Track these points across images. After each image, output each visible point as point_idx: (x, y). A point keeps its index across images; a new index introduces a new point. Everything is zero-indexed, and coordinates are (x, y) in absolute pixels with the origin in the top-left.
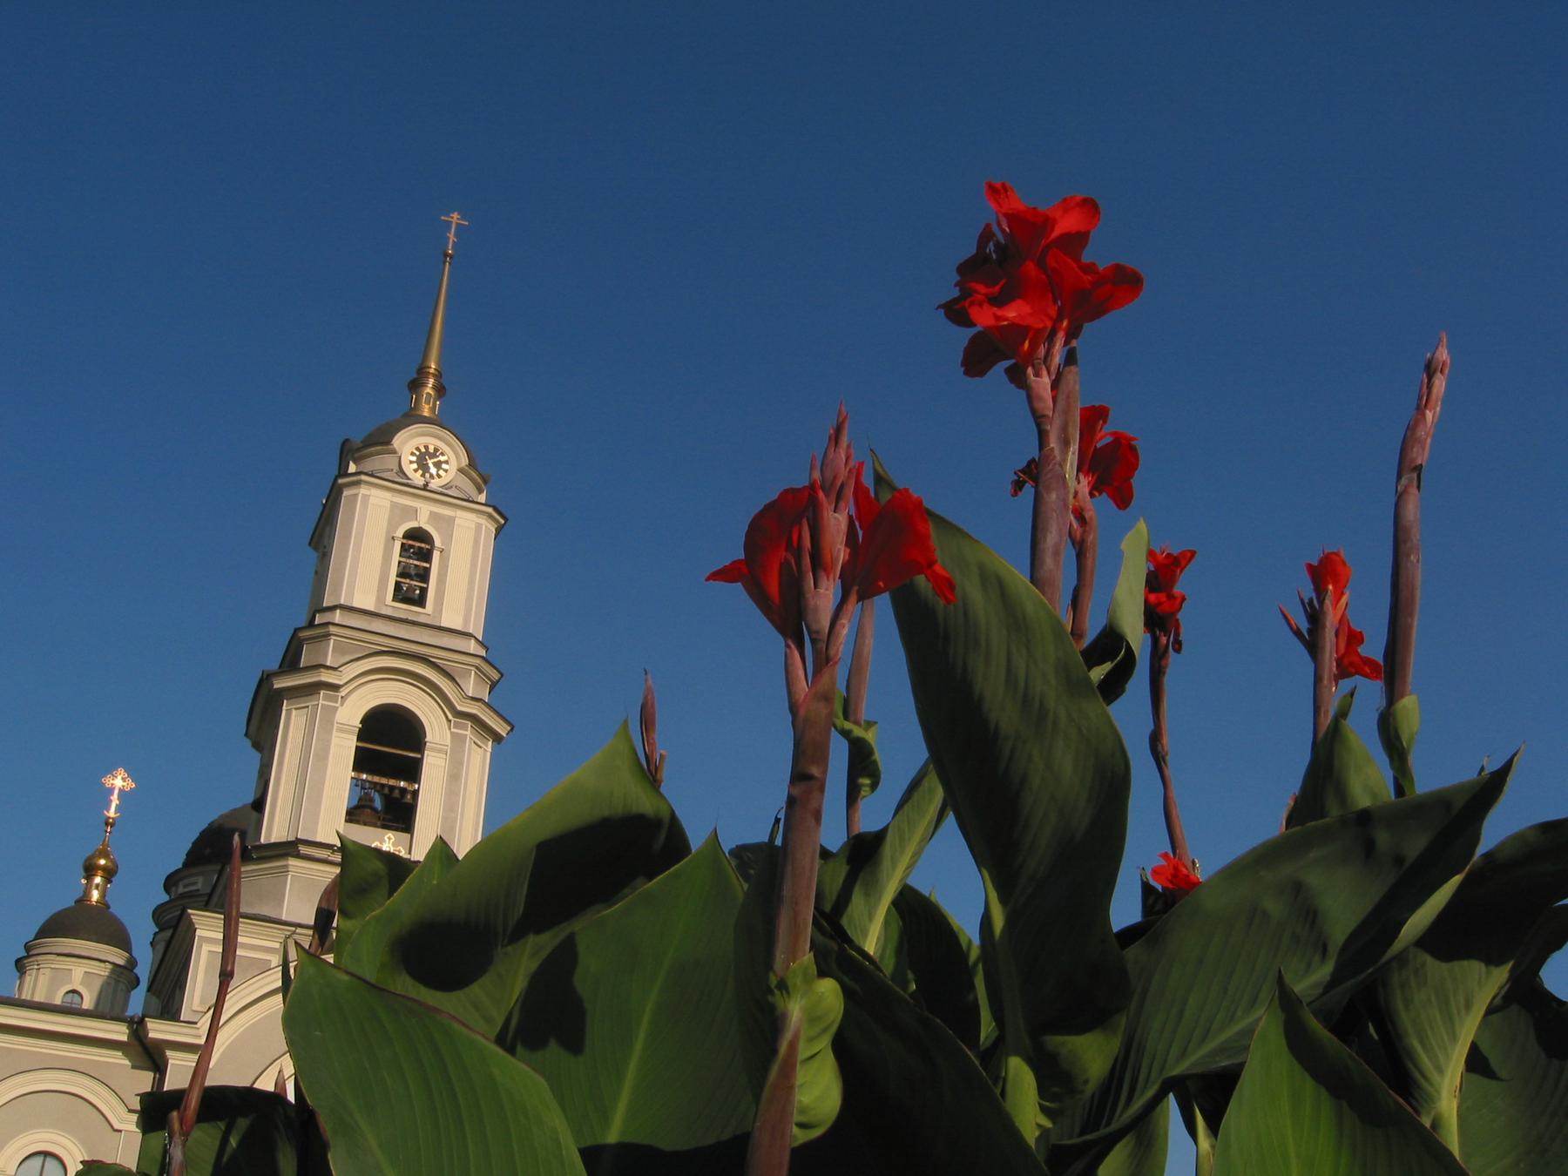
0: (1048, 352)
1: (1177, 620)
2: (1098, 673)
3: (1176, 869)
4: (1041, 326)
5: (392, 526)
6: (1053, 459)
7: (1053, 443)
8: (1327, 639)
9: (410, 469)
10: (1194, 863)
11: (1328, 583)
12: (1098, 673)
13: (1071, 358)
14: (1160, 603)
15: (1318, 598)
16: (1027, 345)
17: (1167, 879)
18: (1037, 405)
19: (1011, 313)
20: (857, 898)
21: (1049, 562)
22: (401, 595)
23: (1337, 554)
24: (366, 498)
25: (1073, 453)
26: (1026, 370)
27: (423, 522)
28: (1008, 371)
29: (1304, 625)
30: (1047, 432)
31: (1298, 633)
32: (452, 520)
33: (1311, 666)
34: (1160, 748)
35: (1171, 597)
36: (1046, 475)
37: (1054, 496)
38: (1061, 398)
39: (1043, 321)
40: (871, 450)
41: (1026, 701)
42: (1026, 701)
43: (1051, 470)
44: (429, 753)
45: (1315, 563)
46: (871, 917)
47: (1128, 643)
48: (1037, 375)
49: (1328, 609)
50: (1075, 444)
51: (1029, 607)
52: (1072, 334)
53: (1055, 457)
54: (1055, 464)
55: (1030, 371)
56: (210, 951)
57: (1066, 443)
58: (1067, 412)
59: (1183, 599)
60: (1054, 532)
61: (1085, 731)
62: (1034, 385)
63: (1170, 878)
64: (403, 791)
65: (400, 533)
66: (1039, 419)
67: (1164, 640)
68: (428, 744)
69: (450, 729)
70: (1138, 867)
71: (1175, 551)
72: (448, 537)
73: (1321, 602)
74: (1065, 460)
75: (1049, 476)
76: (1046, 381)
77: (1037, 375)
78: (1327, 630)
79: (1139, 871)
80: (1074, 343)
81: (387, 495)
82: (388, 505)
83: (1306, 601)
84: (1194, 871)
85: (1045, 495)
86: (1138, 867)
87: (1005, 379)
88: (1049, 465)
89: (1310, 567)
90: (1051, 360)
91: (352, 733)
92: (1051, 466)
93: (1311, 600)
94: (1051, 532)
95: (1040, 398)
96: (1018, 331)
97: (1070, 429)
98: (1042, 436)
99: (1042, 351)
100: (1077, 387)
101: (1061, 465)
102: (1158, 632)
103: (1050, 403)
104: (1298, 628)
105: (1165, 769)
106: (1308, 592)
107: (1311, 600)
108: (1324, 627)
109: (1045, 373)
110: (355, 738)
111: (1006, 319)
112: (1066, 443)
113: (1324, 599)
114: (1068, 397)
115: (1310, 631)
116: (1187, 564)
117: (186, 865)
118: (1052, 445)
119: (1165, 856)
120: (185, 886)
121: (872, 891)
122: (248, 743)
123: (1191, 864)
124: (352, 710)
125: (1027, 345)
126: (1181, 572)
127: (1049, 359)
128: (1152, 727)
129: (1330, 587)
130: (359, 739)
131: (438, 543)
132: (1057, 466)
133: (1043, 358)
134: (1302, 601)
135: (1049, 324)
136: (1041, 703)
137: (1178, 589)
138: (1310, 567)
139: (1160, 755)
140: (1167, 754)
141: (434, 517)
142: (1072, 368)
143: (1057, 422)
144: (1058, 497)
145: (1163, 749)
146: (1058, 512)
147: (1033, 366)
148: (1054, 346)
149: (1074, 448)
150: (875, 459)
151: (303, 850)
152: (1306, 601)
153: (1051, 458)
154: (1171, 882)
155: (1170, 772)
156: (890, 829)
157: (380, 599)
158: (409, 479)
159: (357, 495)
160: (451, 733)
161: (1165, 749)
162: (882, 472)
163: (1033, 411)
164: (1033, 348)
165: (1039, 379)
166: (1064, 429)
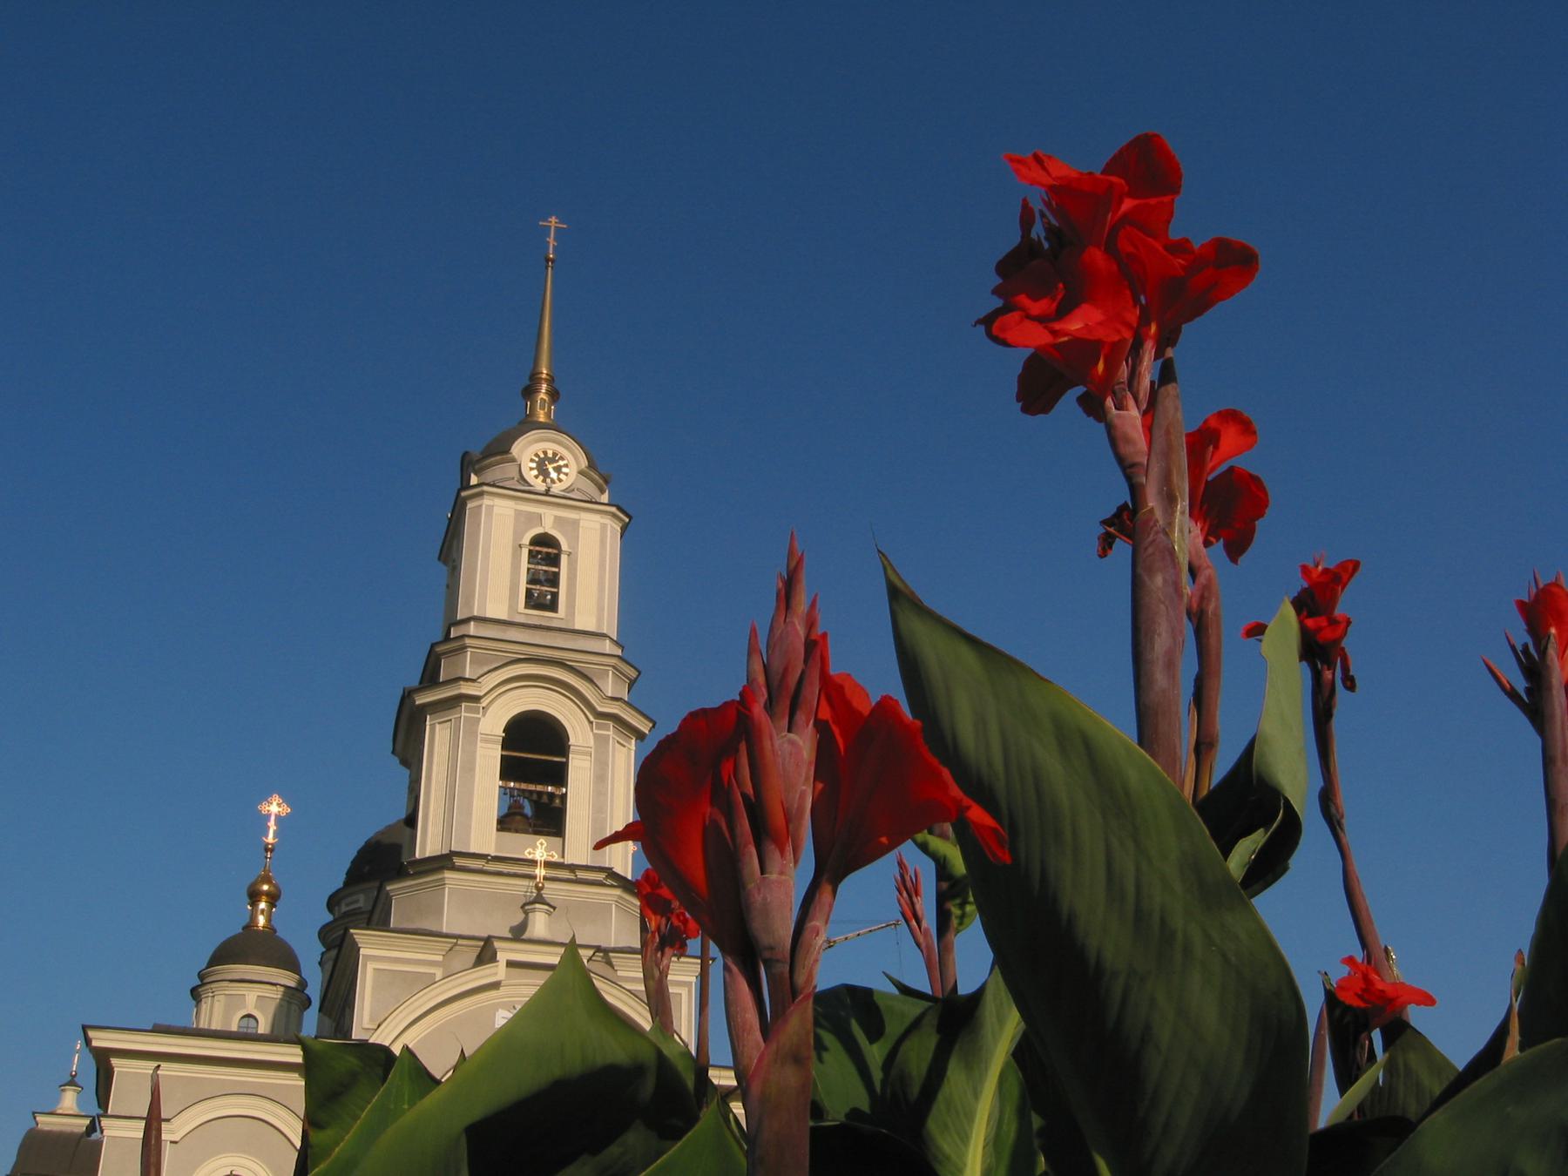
0: (1134, 374)
1: (1343, 649)
2: (1247, 848)
3: (1366, 978)
4: (1116, 338)
5: (518, 534)
6: (1152, 528)
7: (1153, 501)
8: (1557, 704)
9: (531, 475)
10: (1386, 950)
11: (1551, 625)
12: (1247, 848)
13: (1167, 374)
14: (1319, 629)
15: (1537, 645)
16: (1101, 366)
17: (1356, 994)
18: (1126, 450)
19: (1074, 325)
20: (955, 1074)
21: (1160, 678)
22: (533, 602)
23: (1556, 584)
24: (490, 508)
25: (1183, 513)
26: (1105, 400)
27: (548, 527)
28: (1082, 401)
29: (1521, 685)
30: (1142, 486)
31: (1512, 694)
32: (576, 523)
33: (1537, 741)
34: (1333, 810)
35: (1333, 622)
36: (1146, 549)
37: (1159, 580)
38: (1158, 434)
39: (1119, 332)
40: (879, 551)
41: (1140, 916)
42: (1140, 916)
43: (1154, 541)
44: (574, 756)
45: (1526, 599)
46: (977, 1095)
47: (1287, 802)
48: (1120, 407)
49: (1552, 660)
50: (1183, 500)
51: (1133, 776)
52: (1167, 339)
53: (1157, 521)
54: (1157, 533)
55: (1109, 402)
56: (374, 969)
57: (1170, 499)
58: (1167, 454)
59: (1349, 622)
60: (1164, 634)
61: (1233, 959)
62: (1117, 422)
63: (1360, 993)
64: (551, 795)
65: (526, 540)
66: (1128, 469)
67: (1328, 674)
68: (571, 747)
69: (592, 731)
70: (1319, 972)
71: (1330, 563)
72: (575, 539)
73: (1543, 653)
74: (1171, 524)
75: (1150, 550)
76: (1134, 413)
77: (1120, 406)
78: (1555, 692)
79: (1320, 978)
80: (1170, 353)
81: (511, 503)
82: (512, 513)
83: (1519, 648)
84: (1388, 961)
85: (1146, 578)
86: (1319, 972)
87: (1079, 411)
88: (1148, 536)
89: (1521, 605)
90: (1139, 383)
91: (494, 742)
92: (1151, 537)
93: (1525, 647)
94: (1159, 635)
95: (1128, 440)
96: (1085, 349)
97: (1175, 478)
98: (1136, 490)
99: (1124, 371)
100: (1179, 415)
101: (1166, 534)
102: (1319, 666)
103: (1142, 444)
104: (1510, 685)
105: (1342, 835)
106: (1521, 637)
107: (1526, 647)
108: (1550, 688)
109: (1131, 403)
110: (500, 747)
111: (1066, 334)
112: (1170, 499)
113: (1546, 648)
114: (1168, 433)
115: (1528, 691)
116: (1349, 579)
117: (347, 884)
118: (1151, 504)
119: (1350, 961)
120: (347, 905)
121: (975, 1062)
122: (396, 760)
123: (1384, 954)
124: (495, 720)
125: (1101, 366)
126: (1343, 588)
127: (1135, 384)
128: (1322, 784)
129: (1553, 631)
130: (503, 748)
131: (564, 547)
132: (1161, 535)
133: (1126, 382)
134: (1513, 648)
135: (1128, 335)
136: (1163, 921)
137: (1340, 610)
138: (1521, 605)
139: (1334, 819)
140: (1342, 817)
141: (557, 519)
142: (1170, 387)
143: (1155, 471)
144: (1165, 581)
145: (1337, 809)
146: (1167, 603)
147: (1114, 394)
148: (1141, 362)
149: (1183, 505)
150: (886, 563)
151: (458, 861)
152: (1519, 648)
153: (1152, 524)
154: (1360, 997)
155: (1349, 837)
156: (989, 997)
157: (512, 606)
158: (531, 486)
159: (481, 506)
160: (595, 735)
161: (1340, 810)
162: (899, 584)
163: (1120, 460)
164: (1111, 368)
165: (1121, 412)
166: (1167, 478)
